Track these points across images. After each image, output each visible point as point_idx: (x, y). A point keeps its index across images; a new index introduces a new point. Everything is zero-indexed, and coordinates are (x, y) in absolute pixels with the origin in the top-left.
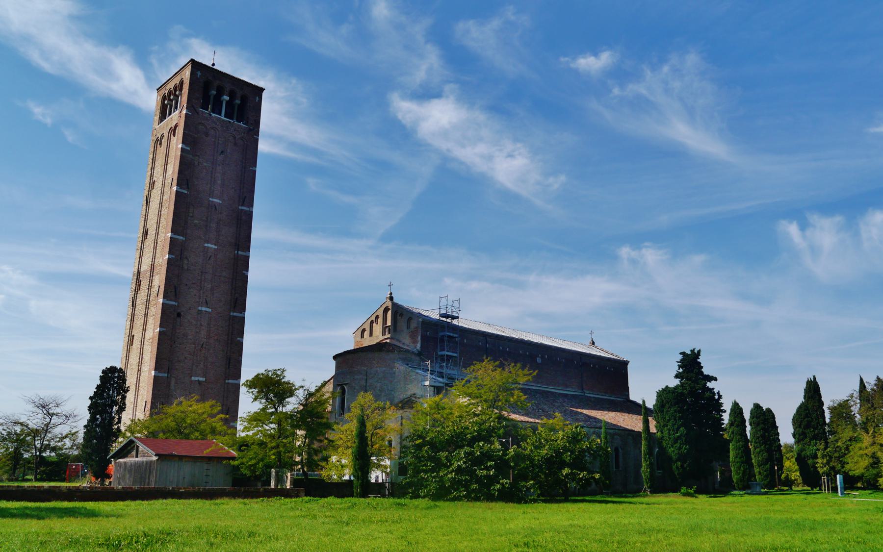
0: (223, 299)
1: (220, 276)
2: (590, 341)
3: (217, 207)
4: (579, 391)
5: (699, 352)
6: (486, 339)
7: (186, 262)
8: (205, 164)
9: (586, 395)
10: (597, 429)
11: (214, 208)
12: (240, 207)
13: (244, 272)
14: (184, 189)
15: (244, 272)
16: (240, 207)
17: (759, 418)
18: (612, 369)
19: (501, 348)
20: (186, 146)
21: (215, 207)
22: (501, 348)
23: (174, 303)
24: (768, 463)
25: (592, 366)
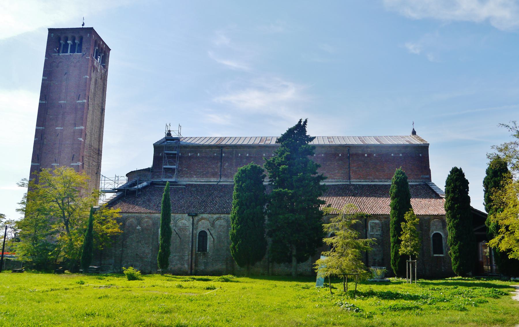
0: (66, 157)
1: (65, 144)
2: (411, 131)
3: (63, 106)
4: (344, 181)
5: (305, 122)
6: (222, 149)
7: (45, 140)
8: (56, 83)
9: (351, 183)
10: (224, 215)
11: (60, 107)
12: (77, 102)
13: (78, 139)
14: (44, 101)
15: (78, 139)
16: (77, 102)
17: (450, 186)
18: (401, 155)
19: (239, 155)
20: (45, 77)
21: (61, 106)
22: (239, 155)
23: (37, 164)
24: (457, 243)
25: (366, 155)
